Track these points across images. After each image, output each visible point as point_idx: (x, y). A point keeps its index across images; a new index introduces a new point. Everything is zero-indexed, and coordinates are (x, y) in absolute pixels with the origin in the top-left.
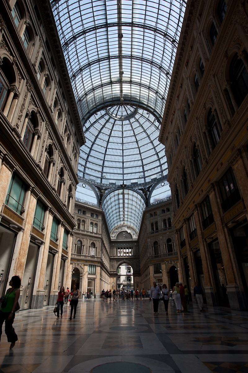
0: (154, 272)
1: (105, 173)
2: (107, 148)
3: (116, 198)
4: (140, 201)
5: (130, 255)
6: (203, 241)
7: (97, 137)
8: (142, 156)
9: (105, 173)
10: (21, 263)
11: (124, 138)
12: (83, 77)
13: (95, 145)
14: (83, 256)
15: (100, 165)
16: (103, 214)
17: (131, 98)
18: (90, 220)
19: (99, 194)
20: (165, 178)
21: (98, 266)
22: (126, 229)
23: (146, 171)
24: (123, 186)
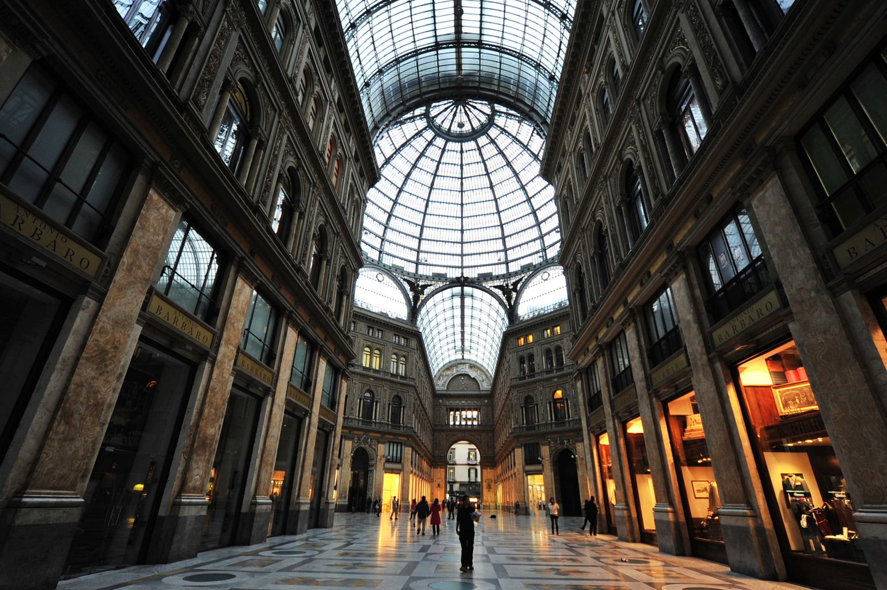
0: (526, 460)
1: (425, 252)
2: (428, 201)
3: (448, 304)
4: (497, 312)
5: (475, 423)
6: (649, 395)
7: (407, 177)
9: (425, 252)
10: (206, 438)
12: (375, 30)
13: (403, 194)
14: (376, 423)
15: (413, 237)
16: (418, 336)
17: (480, 82)
18: (391, 349)
19: (411, 297)
21: (406, 445)
22: (466, 369)
23: (510, 249)
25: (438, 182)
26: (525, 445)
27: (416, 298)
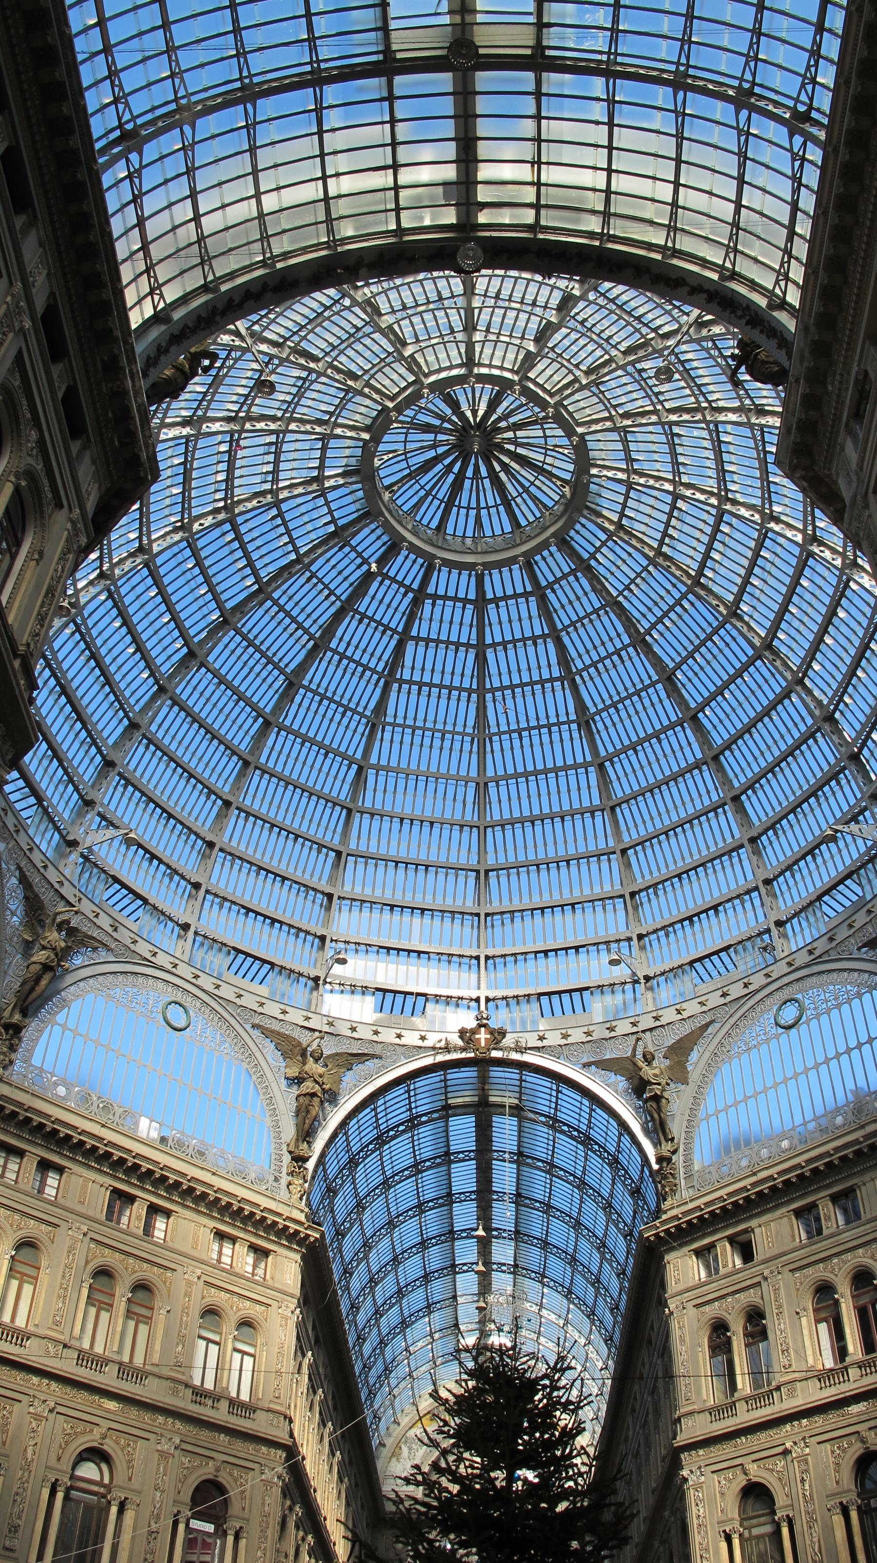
8: (623, 827)
11: (489, 696)
20: (807, 965)
24: (483, 1036)
25: (399, 704)
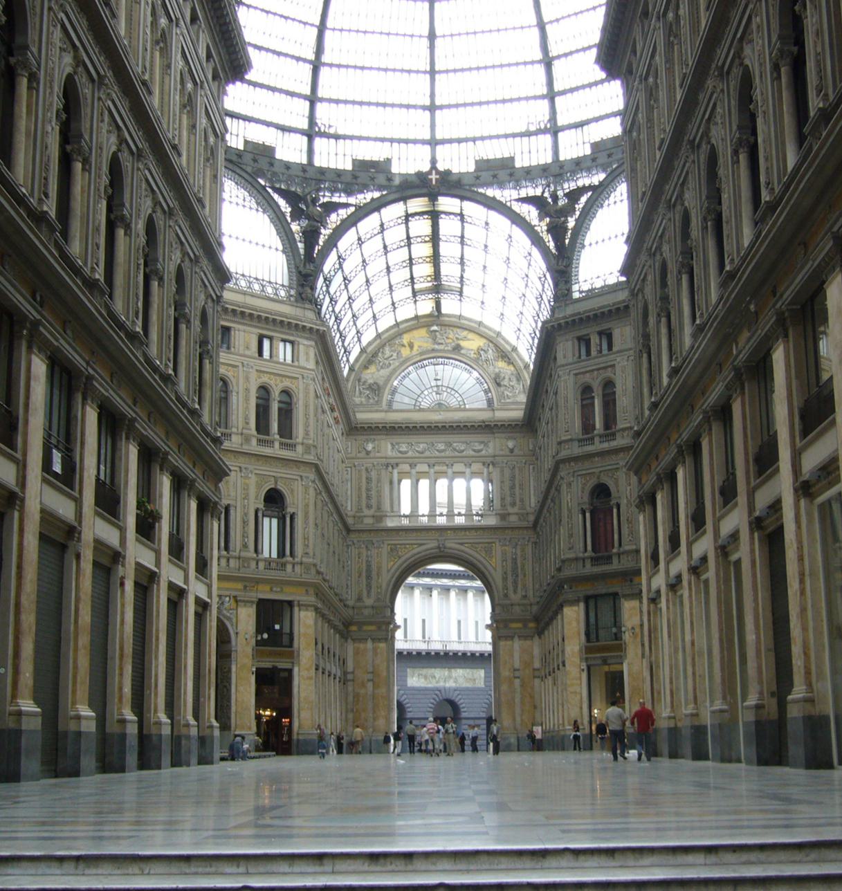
0: (587, 634)
3: (396, 235)
18: (253, 375)
24: (434, 177)
26: (587, 599)
27: (311, 236)
